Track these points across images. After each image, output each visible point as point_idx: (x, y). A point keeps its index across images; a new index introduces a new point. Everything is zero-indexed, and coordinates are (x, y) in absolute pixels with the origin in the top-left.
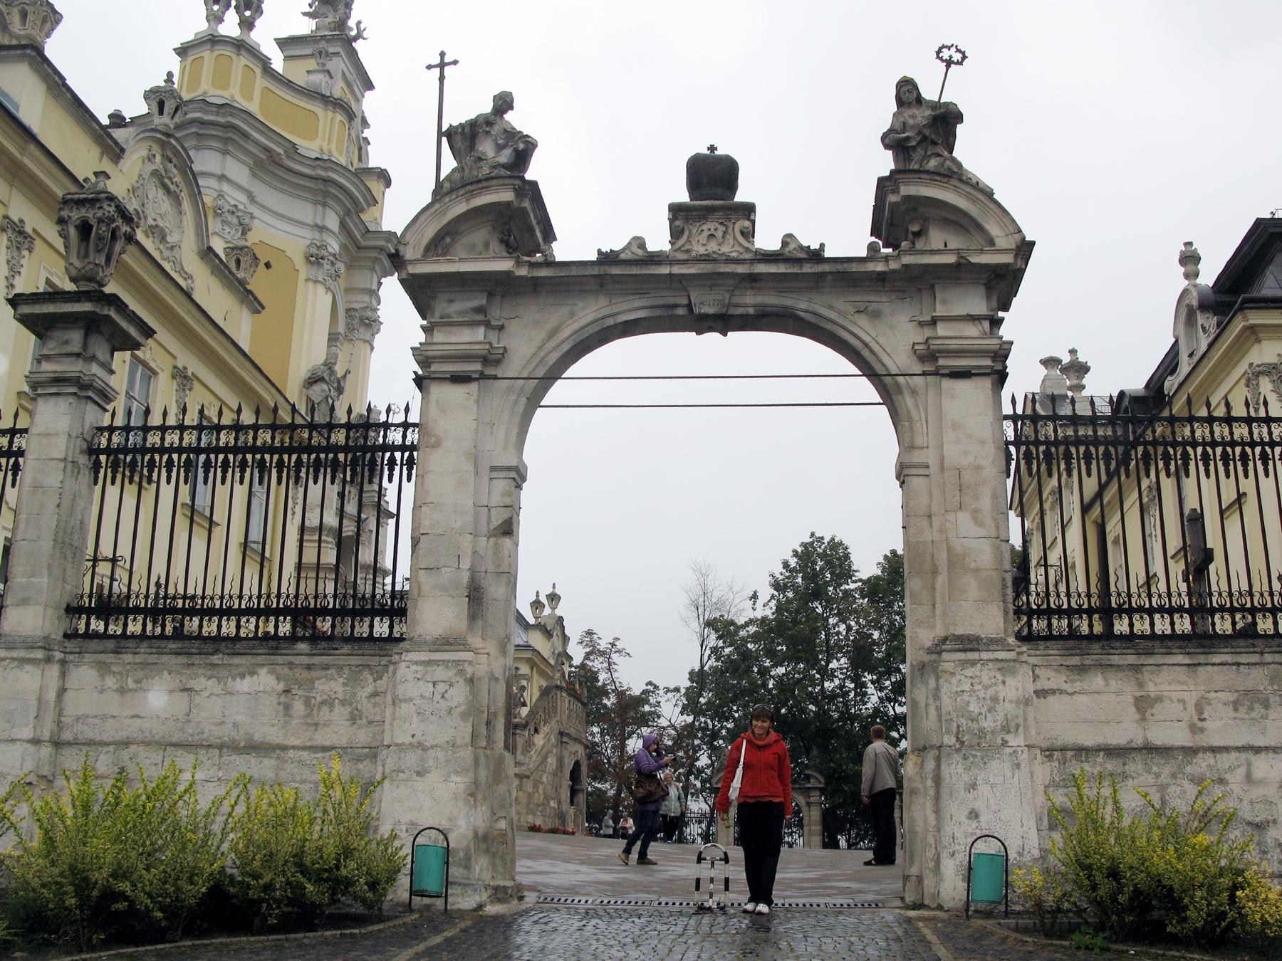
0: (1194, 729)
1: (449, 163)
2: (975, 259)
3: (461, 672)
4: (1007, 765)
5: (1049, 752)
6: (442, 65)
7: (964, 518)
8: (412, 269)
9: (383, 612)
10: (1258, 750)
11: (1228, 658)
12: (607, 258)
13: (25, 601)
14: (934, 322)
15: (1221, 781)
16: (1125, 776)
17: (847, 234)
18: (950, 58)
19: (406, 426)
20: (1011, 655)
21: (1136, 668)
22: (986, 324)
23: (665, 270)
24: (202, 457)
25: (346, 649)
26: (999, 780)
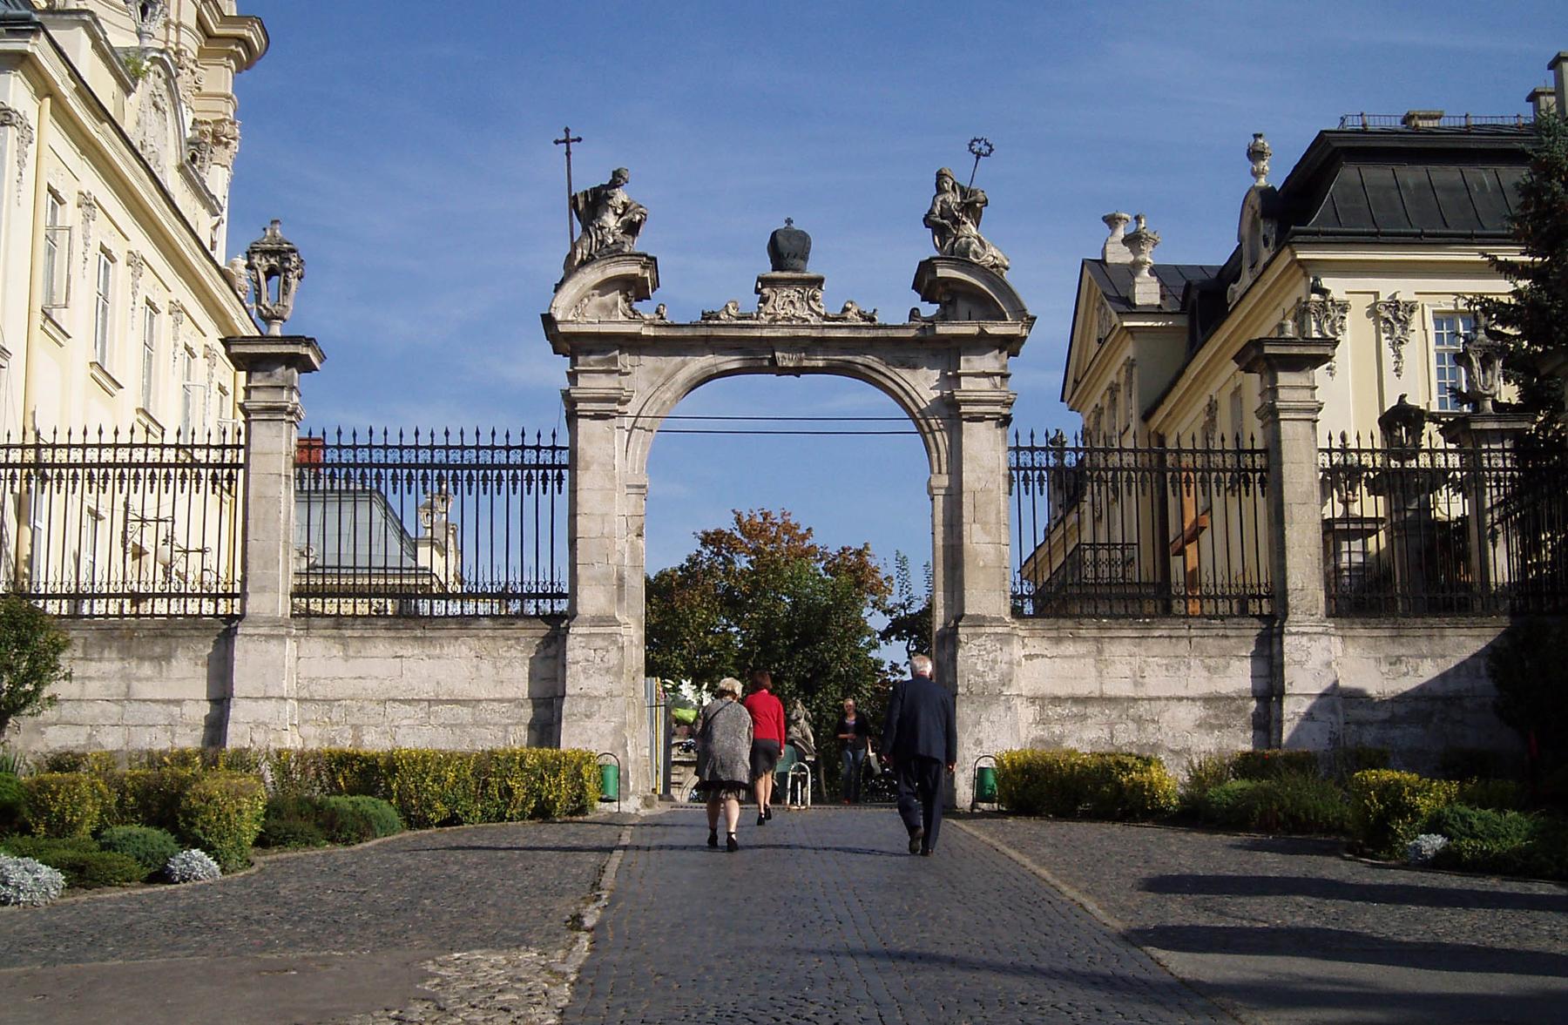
0: (1136, 684)
1: (578, 226)
2: (991, 330)
3: (615, 642)
4: (1002, 708)
5: (1032, 700)
6: (567, 141)
7: (976, 527)
8: (561, 328)
9: (545, 596)
10: (1180, 699)
11: (1165, 633)
12: (707, 316)
13: (263, 589)
14: (958, 377)
15: (1153, 721)
16: (1084, 717)
17: (897, 307)
18: (980, 151)
19: (554, 448)
20: (1005, 630)
21: (1096, 639)
22: (998, 379)
23: (757, 333)
24: (390, 471)
25: (520, 623)
26: (996, 719)
